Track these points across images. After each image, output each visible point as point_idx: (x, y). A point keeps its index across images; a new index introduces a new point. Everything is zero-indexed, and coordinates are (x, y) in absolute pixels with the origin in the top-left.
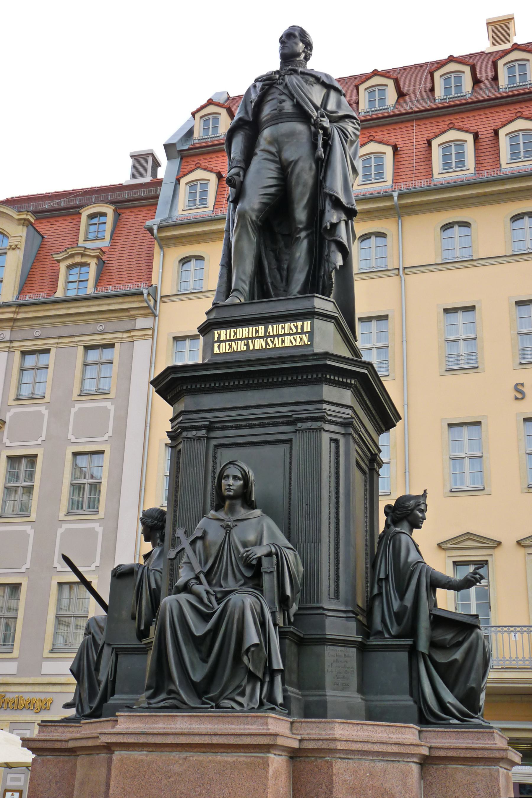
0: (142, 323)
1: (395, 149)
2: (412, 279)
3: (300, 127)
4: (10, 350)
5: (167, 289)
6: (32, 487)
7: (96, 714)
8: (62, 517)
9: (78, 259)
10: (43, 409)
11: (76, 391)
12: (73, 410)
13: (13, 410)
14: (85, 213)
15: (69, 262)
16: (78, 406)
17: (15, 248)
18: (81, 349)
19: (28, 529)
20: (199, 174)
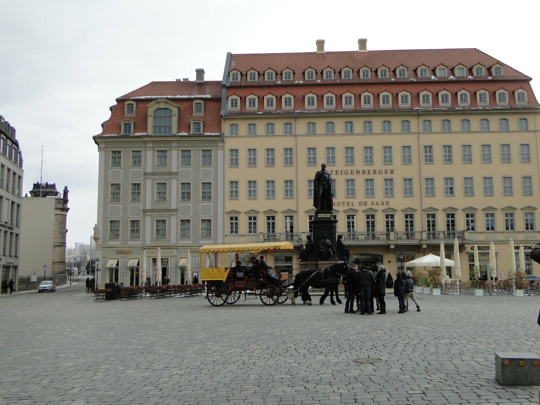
0: (220, 144)
1: (294, 96)
2: (299, 139)
3: (326, 182)
4: (178, 150)
6: (190, 192)
7: (306, 260)
8: (200, 201)
9: (197, 121)
10: (191, 169)
11: (201, 164)
12: (201, 170)
13: (181, 169)
14: (195, 102)
15: (194, 122)
16: (202, 169)
17: (176, 115)
18: (201, 151)
19: (190, 204)
20: (234, 97)
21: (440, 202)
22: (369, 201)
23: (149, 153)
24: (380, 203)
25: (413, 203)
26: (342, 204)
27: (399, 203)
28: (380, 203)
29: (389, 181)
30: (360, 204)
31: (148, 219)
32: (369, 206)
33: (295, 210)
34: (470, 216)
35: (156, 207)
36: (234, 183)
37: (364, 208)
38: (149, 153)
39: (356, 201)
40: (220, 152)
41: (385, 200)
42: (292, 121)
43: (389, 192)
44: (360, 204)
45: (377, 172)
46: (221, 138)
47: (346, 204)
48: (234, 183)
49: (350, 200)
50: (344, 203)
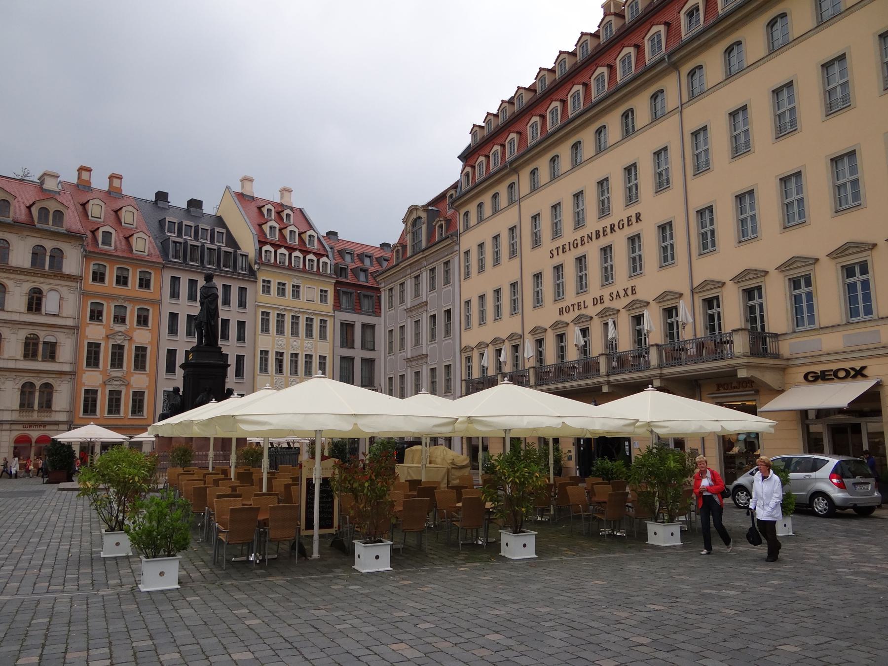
0: (456, 248)
5: (462, 231)
21: (727, 262)
22: (606, 293)
23: (409, 281)
24: (622, 293)
25: (675, 279)
26: (571, 308)
27: (653, 283)
28: (622, 293)
29: (634, 240)
30: (595, 302)
31: (409, 370)
32: (607, 304)
33: (520, 332)
34: (800, 282)
35: (415, 355)
36: (468, 303)
37: (599, 308)
38: (409, 281)
39: (588, 299)
40: (457, 259)
41: (629, 285)
42: (513, 179)
43: (636, 265)
44: (595, 302)
45: (616, 228)
46: (457, 235)
47: (576, 307)
48: (468, 303)
49: (581, 299)
50: (573, 305)
